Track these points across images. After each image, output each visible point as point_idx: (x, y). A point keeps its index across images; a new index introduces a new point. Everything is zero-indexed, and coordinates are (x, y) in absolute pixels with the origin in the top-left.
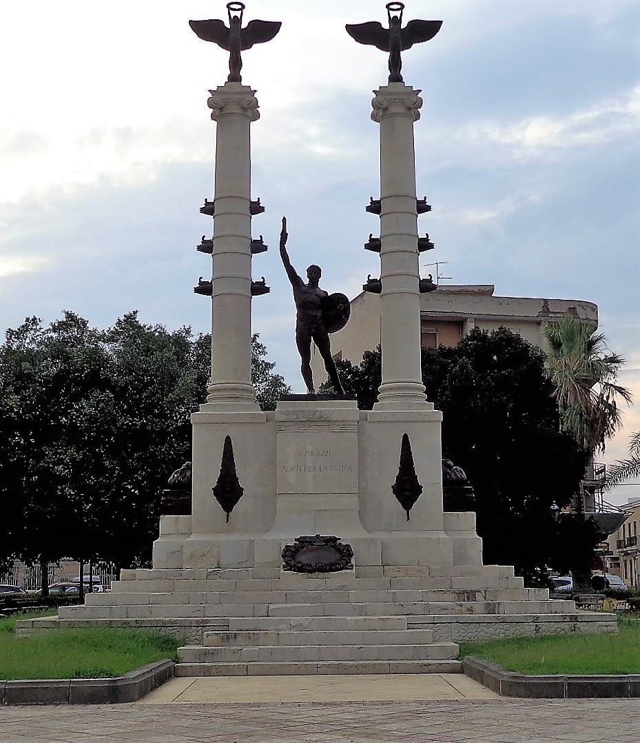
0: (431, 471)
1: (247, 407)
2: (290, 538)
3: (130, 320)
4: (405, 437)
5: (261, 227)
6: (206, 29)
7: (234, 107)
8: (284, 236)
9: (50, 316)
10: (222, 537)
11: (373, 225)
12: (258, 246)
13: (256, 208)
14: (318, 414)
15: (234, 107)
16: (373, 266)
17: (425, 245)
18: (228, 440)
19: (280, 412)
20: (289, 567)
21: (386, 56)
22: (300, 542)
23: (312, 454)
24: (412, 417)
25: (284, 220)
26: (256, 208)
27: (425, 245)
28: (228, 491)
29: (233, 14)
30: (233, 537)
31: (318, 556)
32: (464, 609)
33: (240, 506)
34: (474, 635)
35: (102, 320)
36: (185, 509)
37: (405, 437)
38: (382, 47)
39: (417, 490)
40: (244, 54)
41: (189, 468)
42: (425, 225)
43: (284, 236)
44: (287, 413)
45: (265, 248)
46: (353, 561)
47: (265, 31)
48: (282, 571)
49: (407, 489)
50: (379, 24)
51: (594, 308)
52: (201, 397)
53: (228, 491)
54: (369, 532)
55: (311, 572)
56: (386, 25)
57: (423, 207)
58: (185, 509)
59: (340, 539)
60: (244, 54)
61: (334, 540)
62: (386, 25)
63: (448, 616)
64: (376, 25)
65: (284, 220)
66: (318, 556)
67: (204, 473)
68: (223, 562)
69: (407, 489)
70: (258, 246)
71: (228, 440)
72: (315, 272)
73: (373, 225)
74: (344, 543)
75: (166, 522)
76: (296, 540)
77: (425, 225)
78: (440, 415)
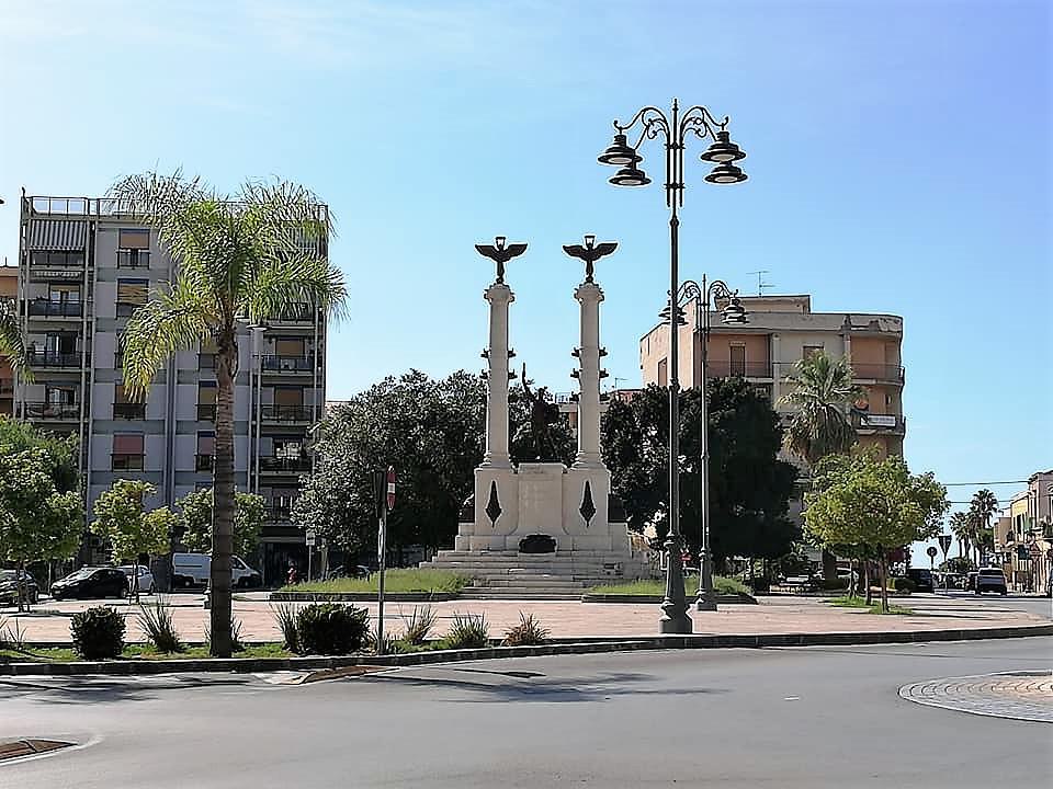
0: (601, 504)
3: (460, 376)
4: (587, 483)
5: (514, 365)
6: (485, 250)
7: (499, 297)
9: (399, 371)
11: (576, 364)
12: (512, 376)
13: (511, 354)
15: (499, 297)
16: (574, 386)
17: (604, 374)
24: (593, 474)
26: (511, 354)
27: (604, 374)
28: (494, 510)
29: (501, 242)
31: (538, 544)
35: (438, 373)
42: (604, 363)
47: (518, 250)
49: (588, 509)
51: (898, 320)
53: (494, 510)
56: (585, 247)
57: (603, 353)
62: (585, 247)
69: (588, 509)
70: (512, 376)
73: (576, 364)
75: (462, 527)
77: (604, 363)
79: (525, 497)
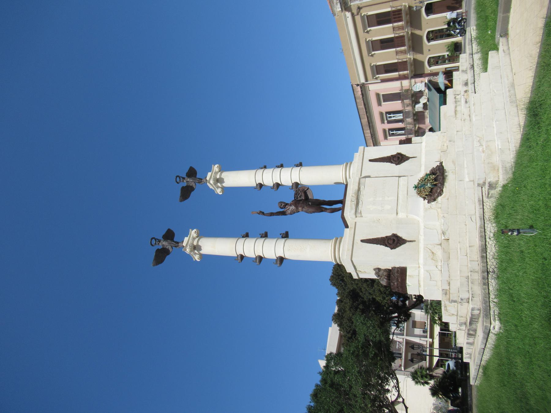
2: (422, 203)
4: (370, 161)
10: (422, 245)
14: (353, 195)
18: (363, 241)
28: (394, 241)
30: (422, 238)
32: (466, 94)
33: (403, 235)
36: (403, 271)
49: (399, 159)
53: (394, 241)
58: (403, 271)
64: (183, 189)
71: (363, 241)
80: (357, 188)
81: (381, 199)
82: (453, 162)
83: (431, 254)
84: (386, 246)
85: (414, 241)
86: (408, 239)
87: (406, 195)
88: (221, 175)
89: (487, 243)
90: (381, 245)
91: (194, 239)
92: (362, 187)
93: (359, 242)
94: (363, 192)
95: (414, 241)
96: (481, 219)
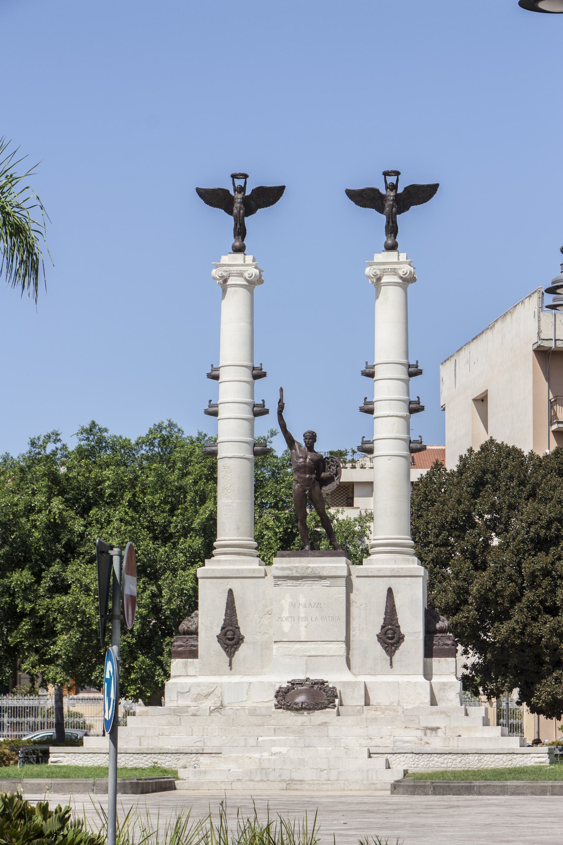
1: (248, 563)
2: (283, 681)
4: (390, 591)
8: (281, 407)
10: (225, 679)
12: (259, 411)
14: (310, 570)
18: (230, 592)
19: (276, 568)
20: (278, 707)
21: (383, 218)
22: (293, 684)
23: (305, 606)
25: (281, 390)
28: (231, 639)
31: (310, 697)
33: (242, 651)
34: (426, 763)
36: (193, 654)
37: (390, 591)
38: (381, 210)
39: (401, 639)
40: (248, 221)
41: (197, 615)
43: (281, 407)
44: (283, 569)
45: (266, 412)
46: (337, 701)
48: (274, 709)
49: (391, 638)
50: (378, 190)
52: (208, 551)
53: (231, 639)
54: (355, 675)
55: (297, 710)
56: (383, 191)
58: (193, 654)
59: (327, 682)
60: (248, 221)
61: (323, 683)
63: (409, 747)
64: (374, 191)
65: (281, 390)
66: (310, 697)
67: (208, 620)
68: (225, 703)
69: (391, 638)
71: (230, 592)
72: (311, 438)
74: (331, 686)
76: (288, 682)
78: (421, 570)
79: (285, 614)
80: (325, 574)
81: (302, 615)
82: (326, 723)
83: (206, 692)
84: (223, 628)
85: (231, 669)
86: (233, 659)
87: (308, 654)
88: (388, 284)
89: (144, 755)
90: (225, 620)
91: (240, 274)
92: (327, 582)
93: (229, 587)
94: (318, 587)
95: (231, 669)
96: (177, 750)
